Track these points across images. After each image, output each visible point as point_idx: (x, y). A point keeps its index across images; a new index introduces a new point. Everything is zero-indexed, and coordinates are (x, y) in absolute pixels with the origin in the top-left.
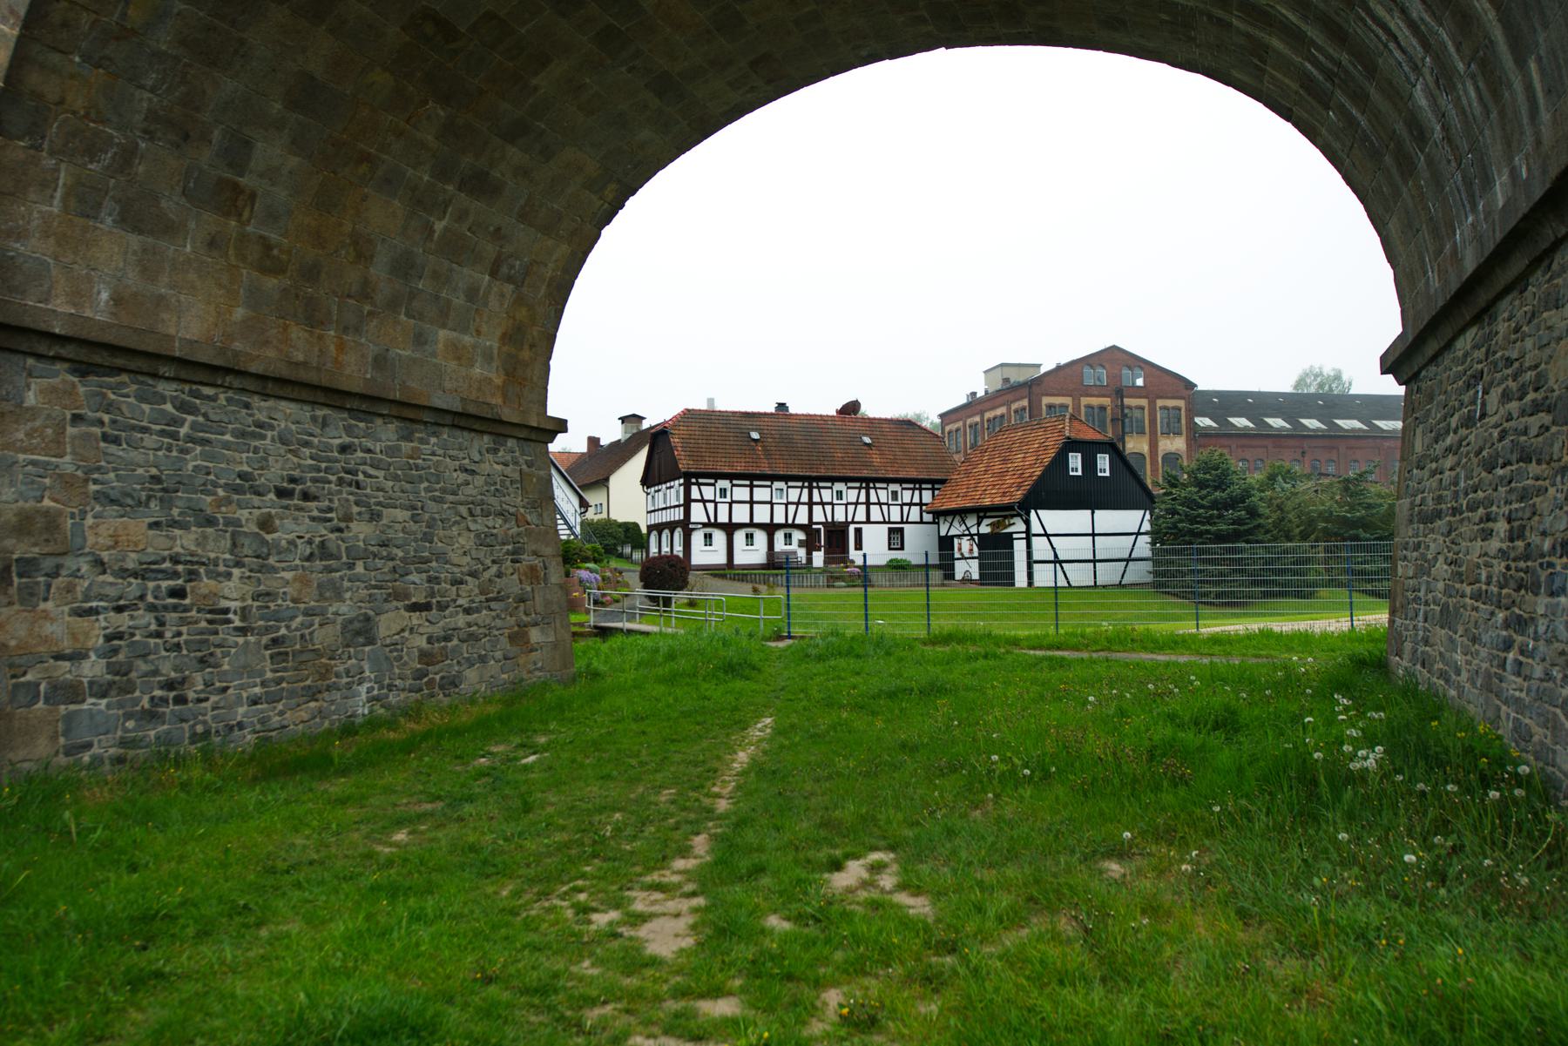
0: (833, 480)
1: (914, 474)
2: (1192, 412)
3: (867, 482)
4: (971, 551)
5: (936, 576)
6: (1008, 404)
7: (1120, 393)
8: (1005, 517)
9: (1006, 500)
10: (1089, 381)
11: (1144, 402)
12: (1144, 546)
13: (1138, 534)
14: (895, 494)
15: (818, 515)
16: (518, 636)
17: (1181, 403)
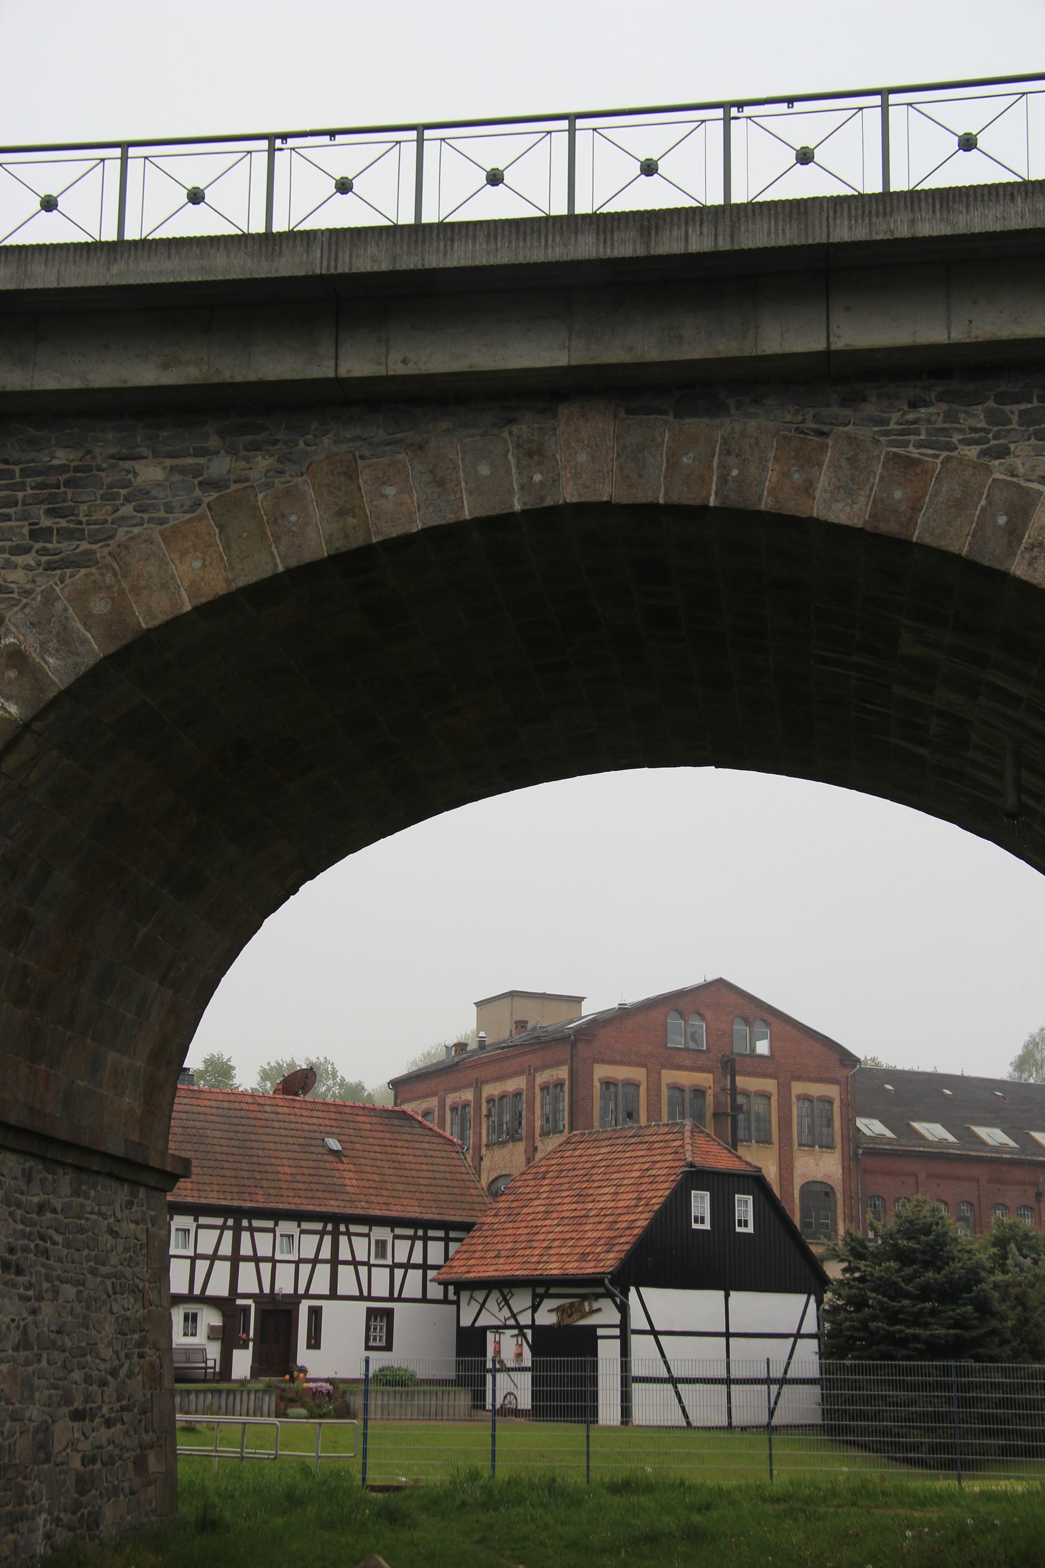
0: (278, 1215)
1: (414, 1212)
2: (852, 1109)
3: (336, 1223)
4: (519, 1355)
5: (463, 1399)
6: (531, 1072)
7: (729, 1066)
8: (584, 1297)
9: (589, 1268)
10: (677, 1041)
11: (769, 1085)
12: (808, 1358)
13: (798, 1336)
14: (381, 1245)
15: (247, 1283)
16: (140, 1464)
17: (833, 1091)
